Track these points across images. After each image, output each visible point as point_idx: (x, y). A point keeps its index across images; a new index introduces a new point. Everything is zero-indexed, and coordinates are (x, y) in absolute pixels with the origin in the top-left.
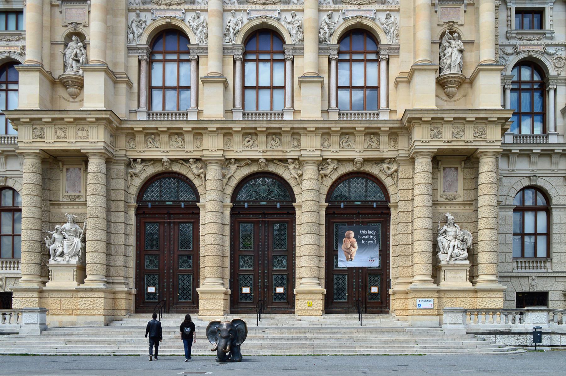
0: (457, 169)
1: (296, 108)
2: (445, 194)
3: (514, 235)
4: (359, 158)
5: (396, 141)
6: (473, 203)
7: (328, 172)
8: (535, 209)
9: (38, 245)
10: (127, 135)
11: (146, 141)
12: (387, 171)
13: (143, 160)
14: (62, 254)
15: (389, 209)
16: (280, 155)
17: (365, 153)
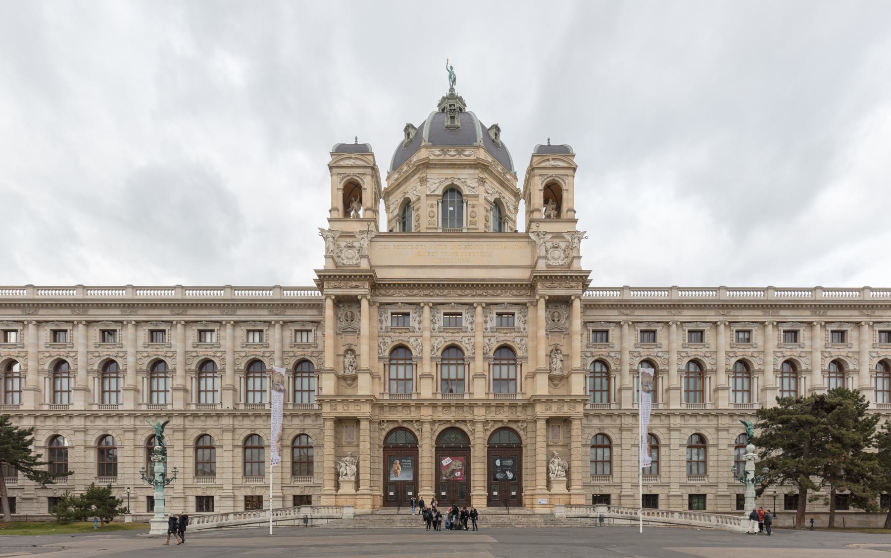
0: (559, 426)
3: (591, 461)
4: (506, 420)
5: (526, 411)
6: (567, 445)
7: (489, 427)
8: (603, 447)
9: (333, 469)
10: (379, 407)
11: (390, 411)
13: (388, 421)
14: (346, 474)
15: (521, 448)
16: (463, 418)
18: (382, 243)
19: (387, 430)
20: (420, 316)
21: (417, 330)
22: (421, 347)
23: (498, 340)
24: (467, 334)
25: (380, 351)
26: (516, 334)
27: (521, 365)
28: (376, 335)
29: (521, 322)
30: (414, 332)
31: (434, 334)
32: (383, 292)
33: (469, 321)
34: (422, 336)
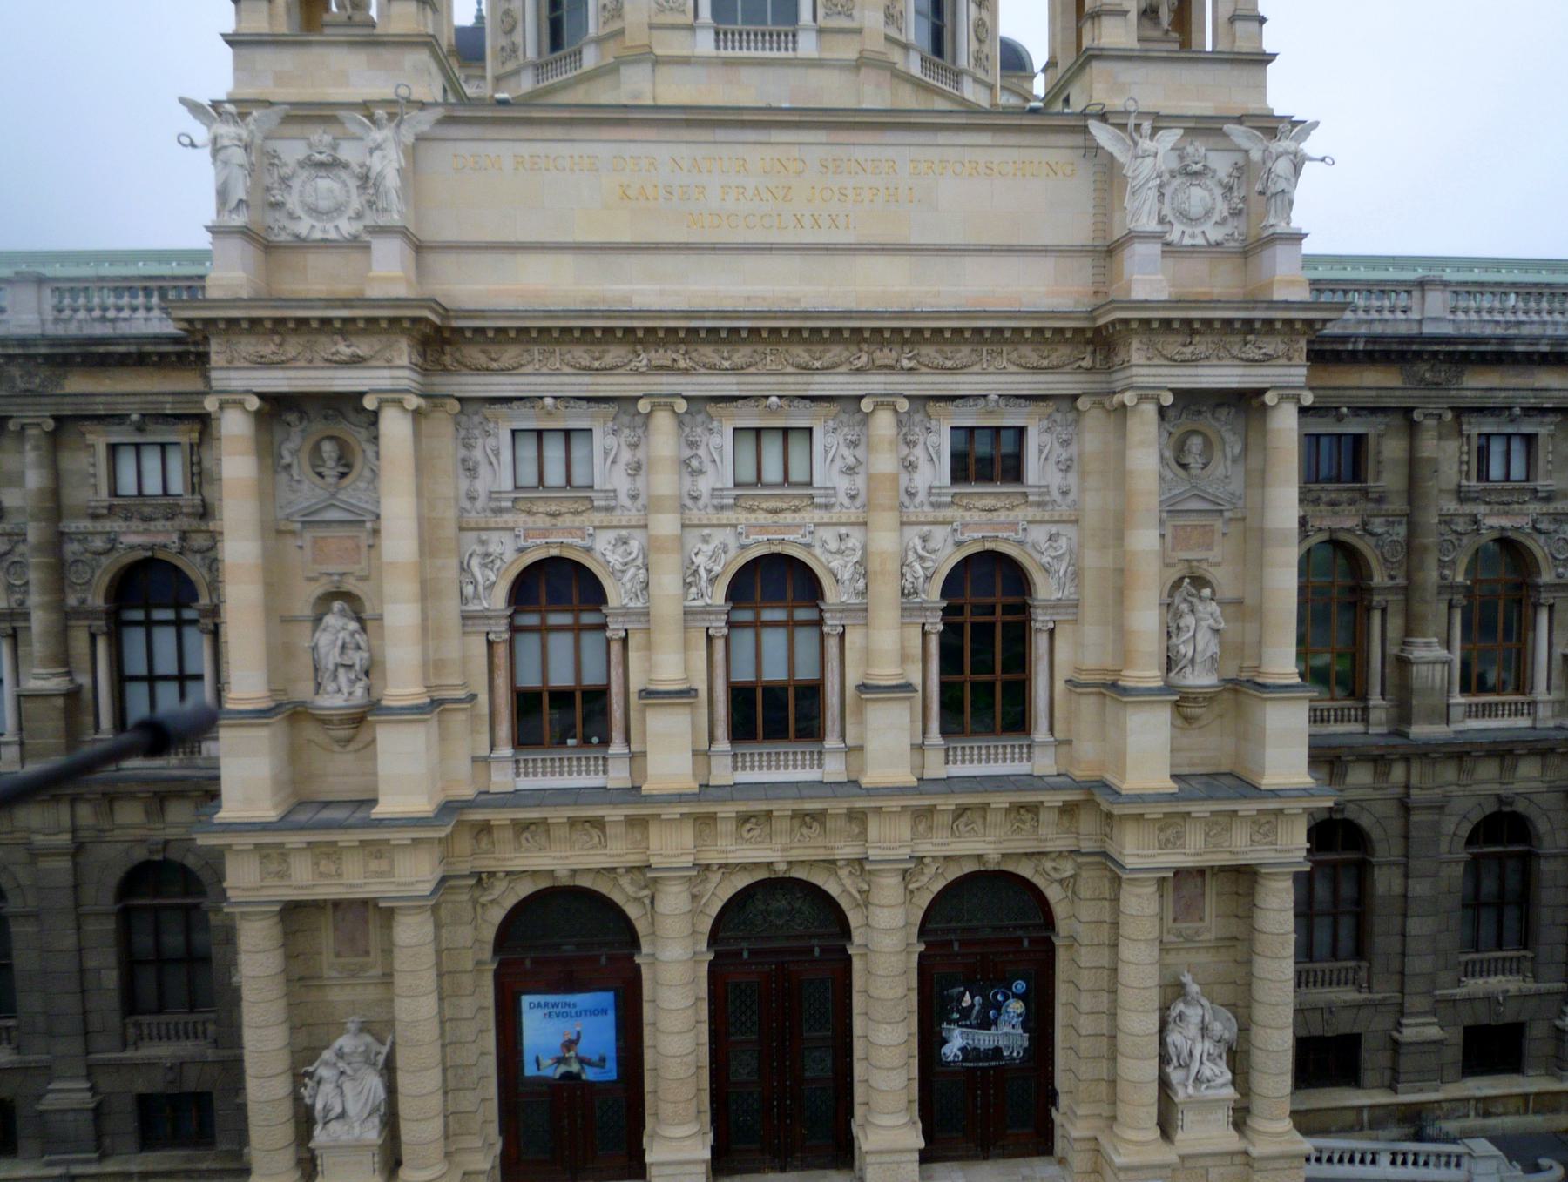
1: (850, 742)
2: (1178, 925)
12: (1052, 873)
13: (508, 873)
16: (822, 854)
17: (1005, 844)
18: (464, 148)
19: (510, 902)
20: (634, 446)
21: (624, 500)
22: (642, 574)
23: (959, 537)
24: (832, 516)
25: (469, 589)
26: (1032, 513)
27: (1052, 632)
28: (450, 530)
29: (1051, 466)
30: (609, 509)
31: (695, 516)
32: (474, 354)
33: (839, 463)
34: (646, 526)
